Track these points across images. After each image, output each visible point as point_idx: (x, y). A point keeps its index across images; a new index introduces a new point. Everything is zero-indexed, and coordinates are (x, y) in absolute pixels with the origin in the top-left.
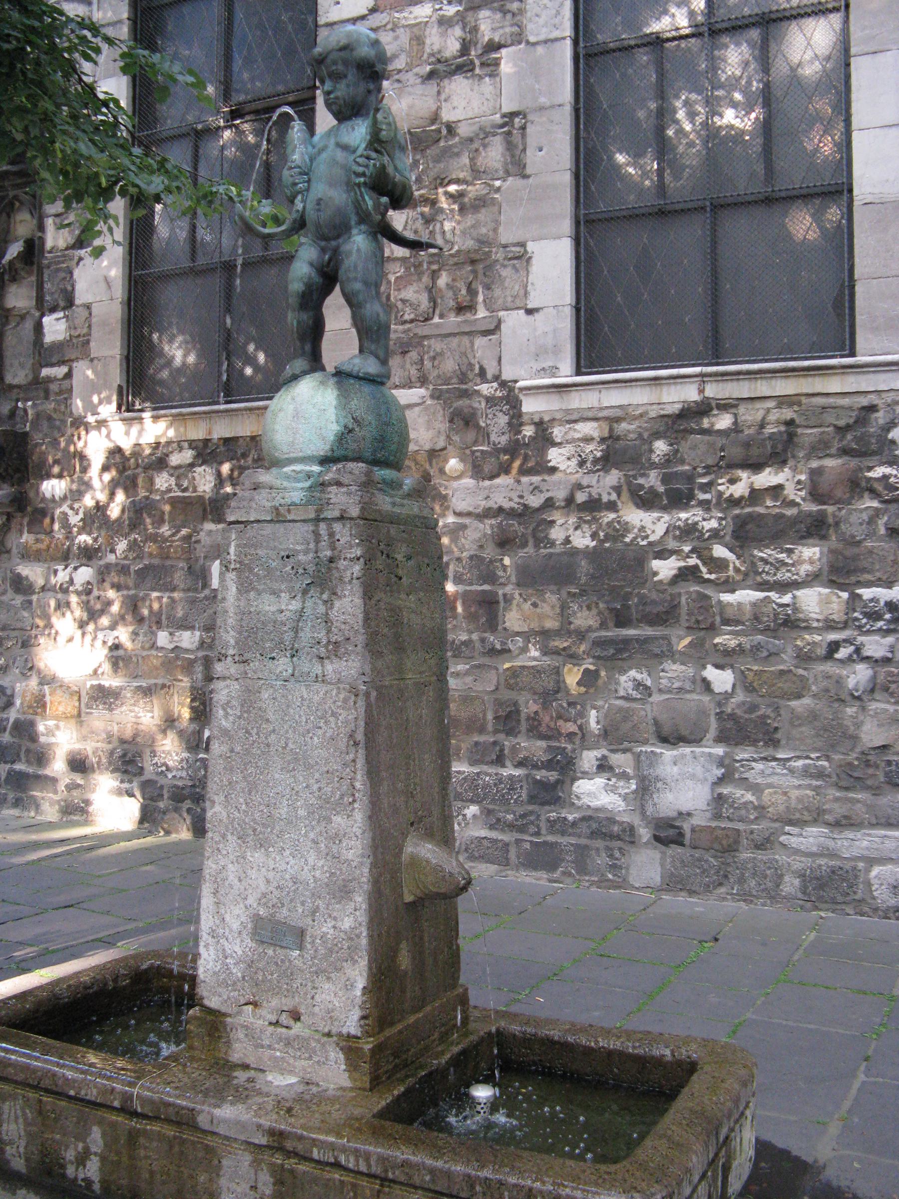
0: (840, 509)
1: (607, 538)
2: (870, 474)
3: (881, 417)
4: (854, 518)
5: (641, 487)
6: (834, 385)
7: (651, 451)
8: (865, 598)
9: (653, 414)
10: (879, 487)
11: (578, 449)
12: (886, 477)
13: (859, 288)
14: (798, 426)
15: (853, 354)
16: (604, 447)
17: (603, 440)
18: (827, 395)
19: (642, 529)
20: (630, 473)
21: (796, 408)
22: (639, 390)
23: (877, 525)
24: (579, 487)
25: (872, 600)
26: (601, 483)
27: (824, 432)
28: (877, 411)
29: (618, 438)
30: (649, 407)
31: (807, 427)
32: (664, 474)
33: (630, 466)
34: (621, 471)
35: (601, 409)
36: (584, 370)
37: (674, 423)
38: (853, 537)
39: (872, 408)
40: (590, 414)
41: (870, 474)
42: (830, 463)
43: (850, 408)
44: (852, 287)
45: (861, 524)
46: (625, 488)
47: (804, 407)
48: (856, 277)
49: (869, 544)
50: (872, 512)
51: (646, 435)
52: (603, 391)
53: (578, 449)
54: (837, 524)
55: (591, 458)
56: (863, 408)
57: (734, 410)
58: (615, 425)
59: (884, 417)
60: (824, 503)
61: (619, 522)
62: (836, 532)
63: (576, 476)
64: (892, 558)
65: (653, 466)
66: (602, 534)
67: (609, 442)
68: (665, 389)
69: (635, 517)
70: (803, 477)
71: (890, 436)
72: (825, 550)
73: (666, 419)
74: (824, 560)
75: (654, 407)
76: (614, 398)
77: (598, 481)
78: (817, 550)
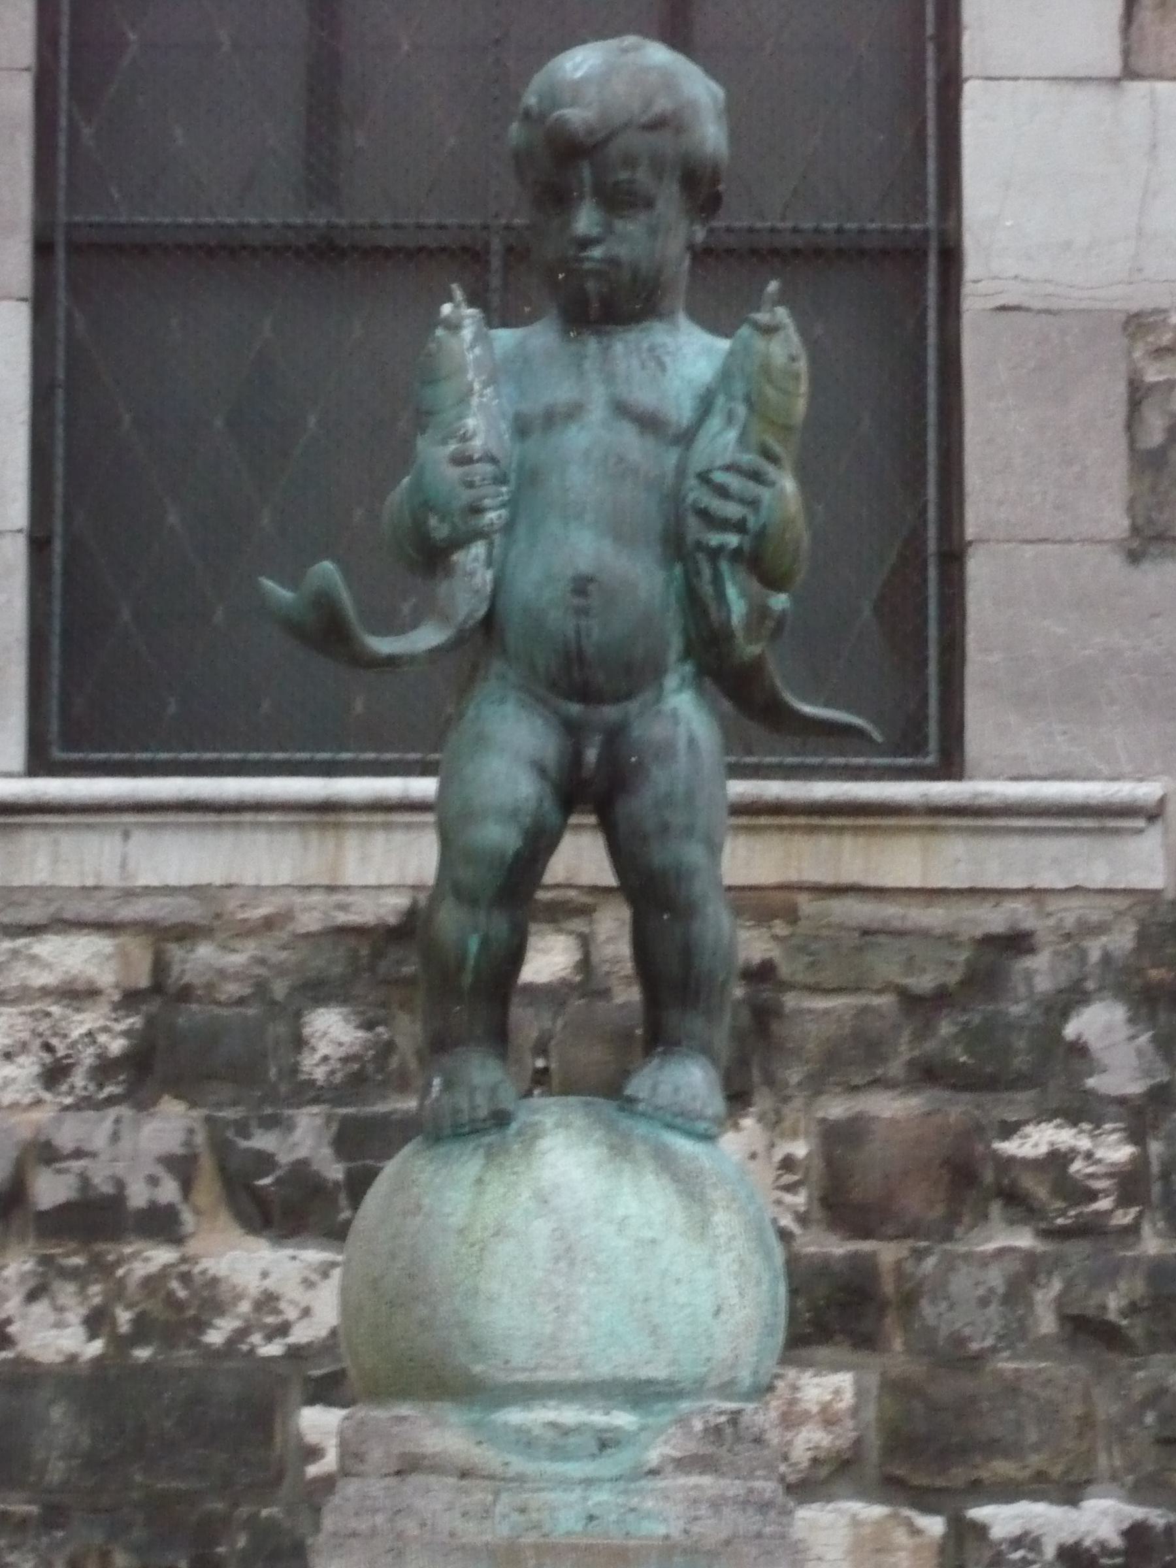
0: (919, 1255)
1: (142, 1330)
2: (1010, 1147)
3: (1041, 971)
4: (961, 1283)
5: (265, 1161)
6: (901, 862)
7: (299, 1042)
8: (998, 1532)
9: (309, 922)
10: (1040, 1191)
11: (44, 1026)
12: (1058, 1159)
13: (979, 570)
14: (786, 986)
15: (951, 765)
16: (134, 1021)
17: (130, 999)
18: (880, 892)
19: (268, 1301)
20: (229, 1114)
21: (780, 928)
22: (262, 837)
23: (1030, 1304)
24: (45, 1153)
25: (1017, 1542)
26: (125, 1145)
27: (865, 1010)
28: (1032, 950)
29: (185, 994)
30: (298, 899)
31: (816, 989)
32: (345, 1121)
33: (226, 1091)
34: (193, 1104)
35: (129, 894)
36: (58, 754)
37: (377, 954)
38: (959, 1341)
39: (1017, 942)
40: (90, 910)
41: (1010, 1147)
42: (889, 1107)
43: (949, 939)
44: (953, 557)
45: (984, 1302)
46: (207, 1164)
47: (803, 927)
48: (970, 532)
49: (1006, 1365)
50: (1014, 1265)
51: (280, 989)
52: (139, 838)
53: (44, 1026)
54: (909, 1301)
55: (88, 1057)
56: (989, 941)
57: (579, 924)
58: (175, 951)
59: (1053, 970)
60: (867, 1234)
61: (186, 1278)
62: (906, 1326)
63: (36, 1115)
64: (1077, 1409)
65: (306, 1092)
66: (124, 1317)
67: (153, 1006)
68: (352, 840)
69: (242, 1261)
70: (800, 1149)
71: (1070, 1030)
72: (873, 1380)
73: (352, 941)
74: (870, 1413)
75: (315, 898)
76: (177, 862)
77: (115, 1137)
78: (844, 1380)
